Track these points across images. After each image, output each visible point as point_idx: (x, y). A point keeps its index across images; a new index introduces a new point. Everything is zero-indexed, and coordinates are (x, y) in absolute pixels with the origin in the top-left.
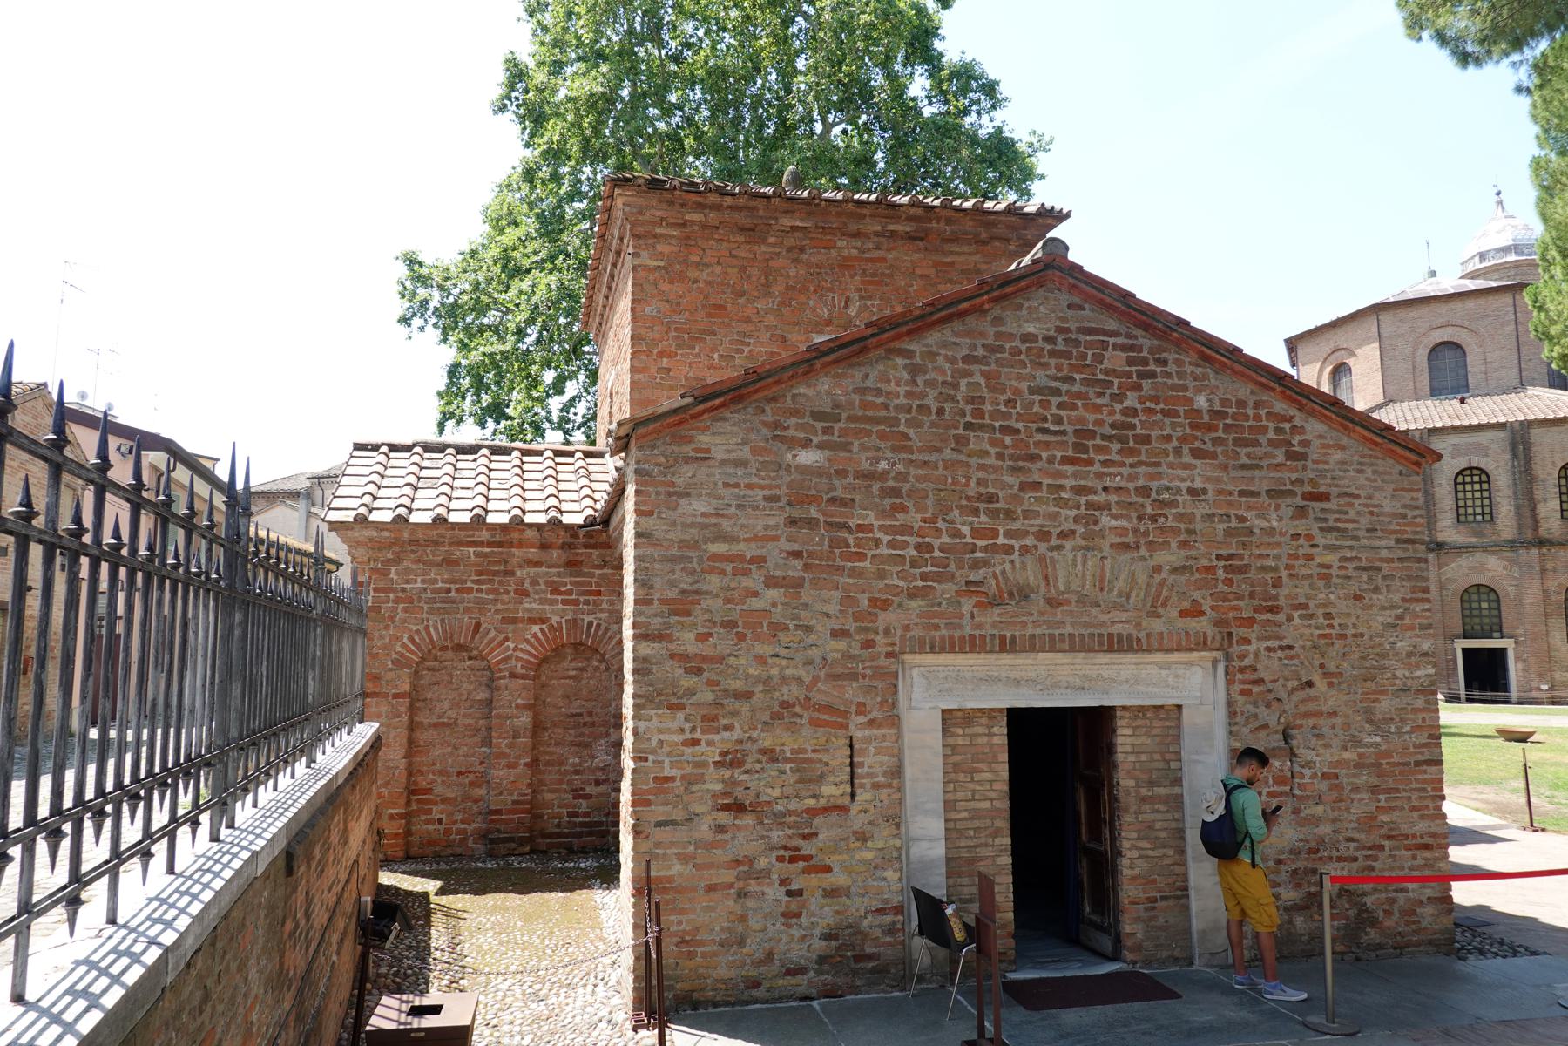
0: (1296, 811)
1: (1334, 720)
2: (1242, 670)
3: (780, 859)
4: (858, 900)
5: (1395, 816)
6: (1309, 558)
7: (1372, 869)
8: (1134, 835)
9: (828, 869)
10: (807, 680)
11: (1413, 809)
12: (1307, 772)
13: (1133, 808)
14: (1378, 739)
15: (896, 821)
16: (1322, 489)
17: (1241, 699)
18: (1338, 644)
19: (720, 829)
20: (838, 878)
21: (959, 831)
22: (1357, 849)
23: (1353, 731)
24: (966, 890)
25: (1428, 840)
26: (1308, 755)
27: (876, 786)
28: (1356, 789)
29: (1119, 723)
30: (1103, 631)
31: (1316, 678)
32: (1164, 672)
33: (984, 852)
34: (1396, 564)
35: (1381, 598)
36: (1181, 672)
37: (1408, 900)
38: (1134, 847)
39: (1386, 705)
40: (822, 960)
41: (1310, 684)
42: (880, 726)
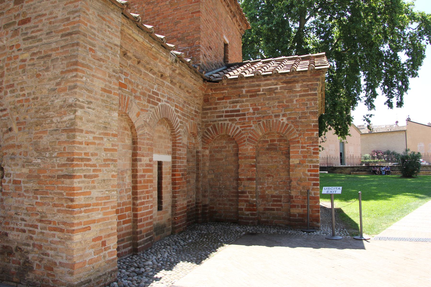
5: (45, 208)
6: (16, 57)
7: (31, 238)
11: (55, 205)
14: (39, 161)
16: (28, 16)
18: (26, 104)
22: (25, 225)
25: (61, 226)
28: (27, 191)
34: (61, 51)
35: (48, 75)
37: (49, 261)
39: (45, 140)
41: (10, 130)
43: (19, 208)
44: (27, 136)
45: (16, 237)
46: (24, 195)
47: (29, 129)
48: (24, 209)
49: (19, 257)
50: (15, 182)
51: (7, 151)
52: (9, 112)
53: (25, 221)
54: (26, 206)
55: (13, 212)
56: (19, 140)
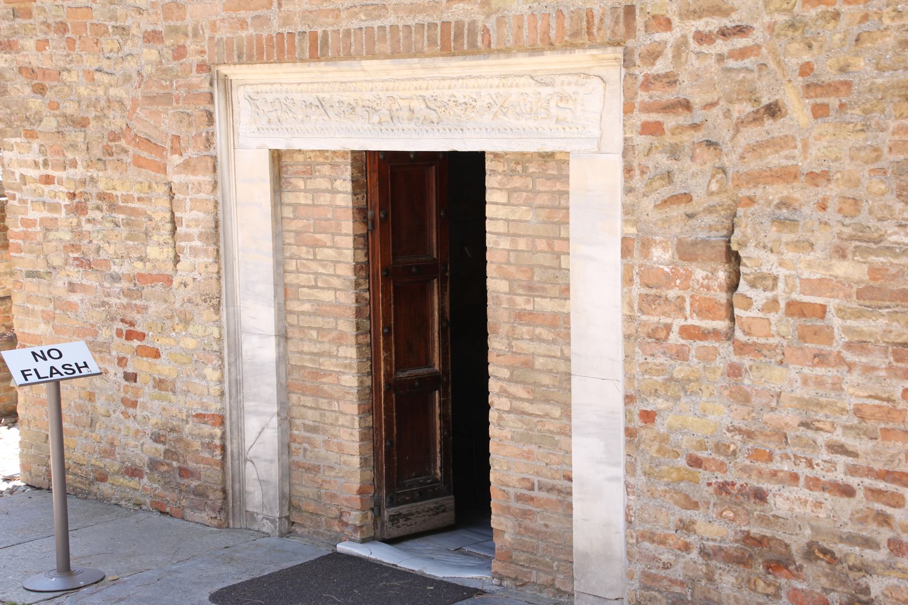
0: (735, 371)
1: (823, 191)
2: (647, 84)
3: (119, 333)
4: (181, 398)
7: (884, 520)
8: (505, 373)
9: (157, 354)
10: (128, 103)
12: (759, 297)
13: (504, 329)
15: (217, 300)
17: (642, 141)
19: (72, 287)
20: (164, 367)
21: (302, 329)
22: (853, 470)
23: (864, 218)
24: (310, 413)
26: (769, 263)
27: (194, 252)
28: (860, 345)
29: (490, 181)
30: (435, 19)
31: (792, 99)
32: (545, 91)
33: (328, 364)
36: (570, 90)
38: (504, 392)
40: (154, 464)
41: (773, 110)
42: (194, 171)
43: (820, 405)
44: (858, 140)
45: (808, 509)
46: (841, 361)
47: (866, 112)
48: (843, 410)
49: (824, 581)
50: (796, 309)
51: (759, 192)
52: (760, 41)
53: (855, 455)
54: (854, 401)
55: (789, 417)
56: (813, 151)
